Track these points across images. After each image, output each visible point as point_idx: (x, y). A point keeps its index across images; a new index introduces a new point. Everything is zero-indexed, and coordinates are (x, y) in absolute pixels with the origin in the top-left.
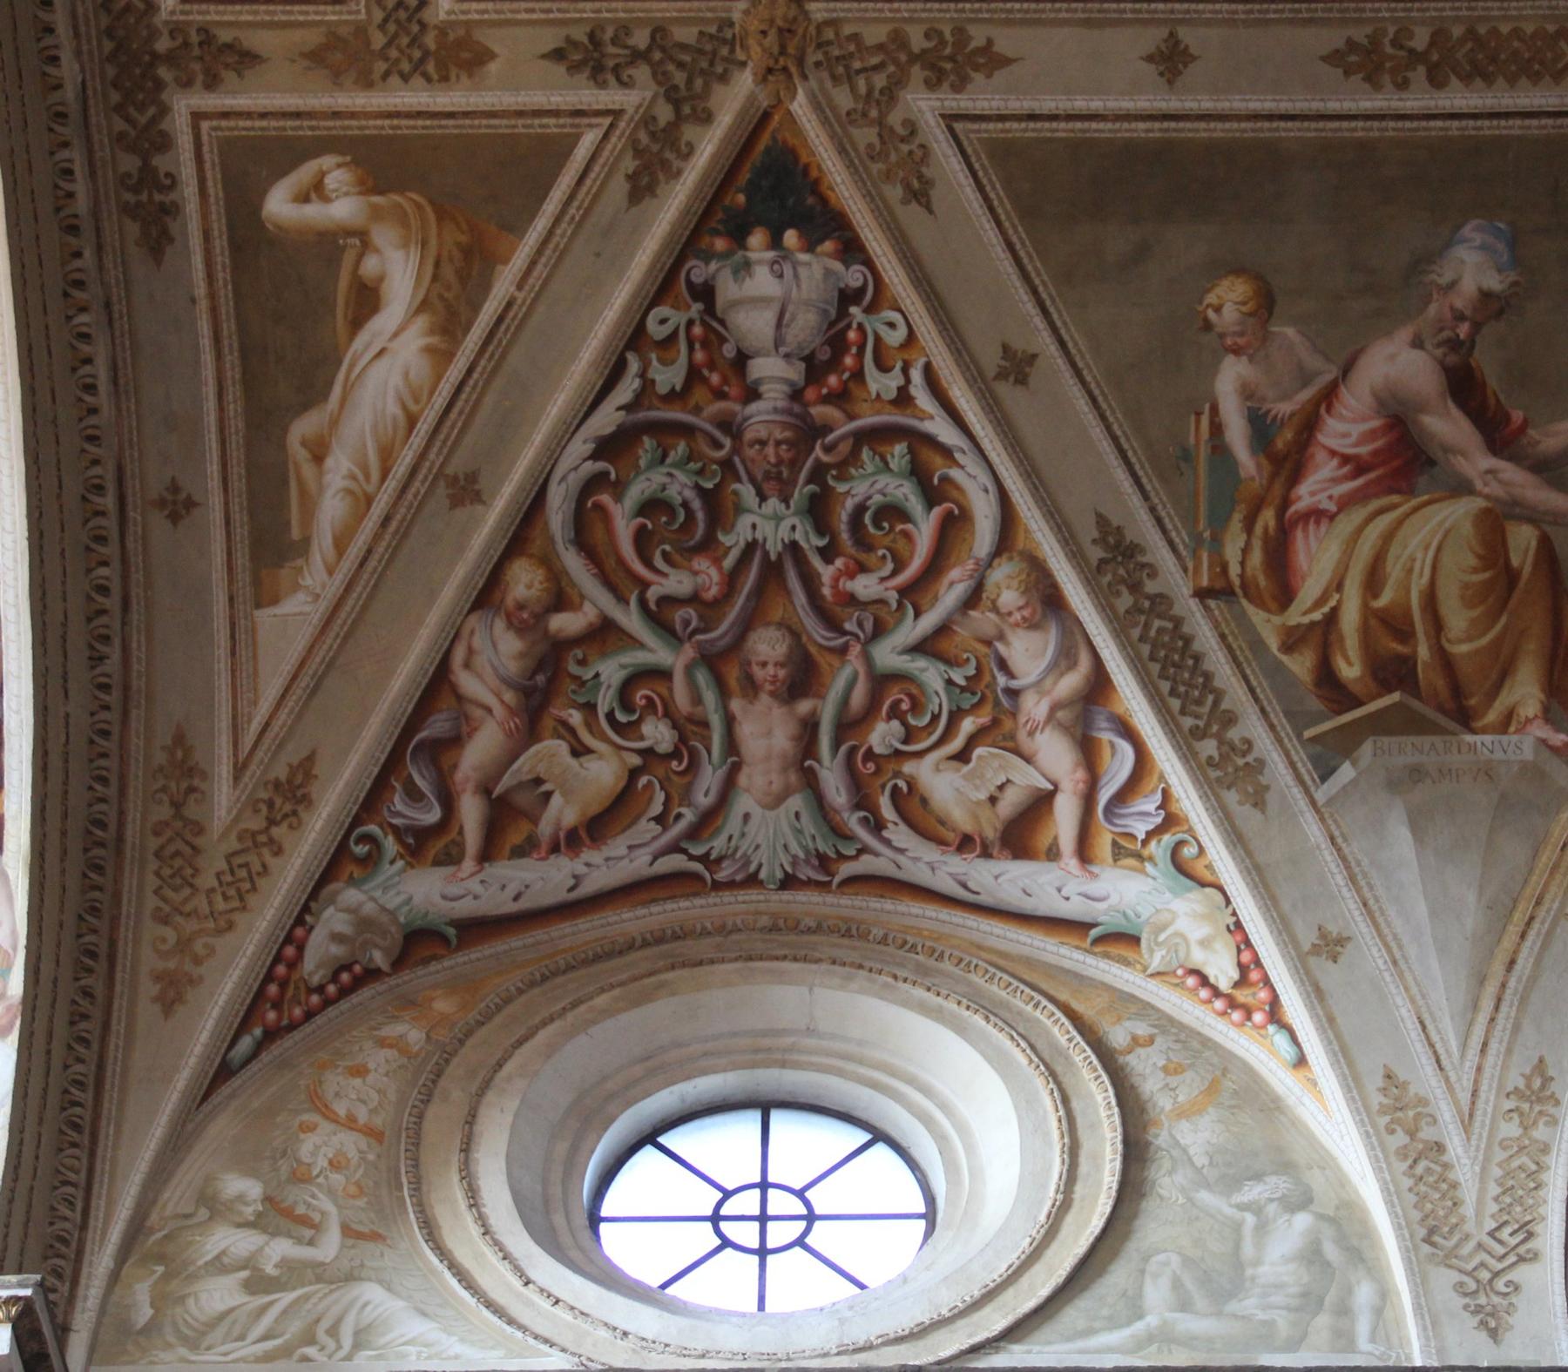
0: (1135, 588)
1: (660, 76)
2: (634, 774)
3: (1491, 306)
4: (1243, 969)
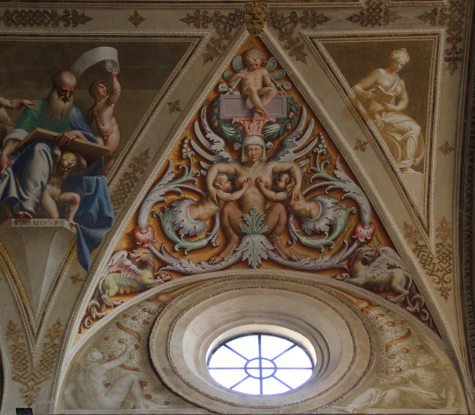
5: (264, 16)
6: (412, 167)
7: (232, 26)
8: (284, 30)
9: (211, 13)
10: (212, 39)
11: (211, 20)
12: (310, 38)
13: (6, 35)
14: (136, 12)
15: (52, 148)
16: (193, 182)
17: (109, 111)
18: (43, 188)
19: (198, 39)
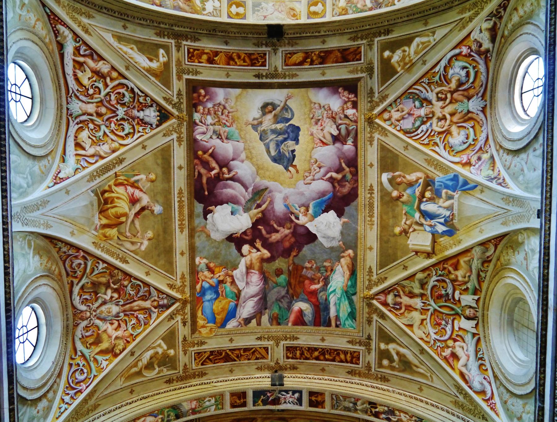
0: (116, 163)
1: (178, 102)
2: (85, 87)
3: (152, 212)
4: (62, 179)
6: (433, 36)
7: (374, 126)
9: (369, 135)
10: (379, 134)
15: (423, 202)
16: (441, 138)
17: (407, 176)
18: (440, 207)
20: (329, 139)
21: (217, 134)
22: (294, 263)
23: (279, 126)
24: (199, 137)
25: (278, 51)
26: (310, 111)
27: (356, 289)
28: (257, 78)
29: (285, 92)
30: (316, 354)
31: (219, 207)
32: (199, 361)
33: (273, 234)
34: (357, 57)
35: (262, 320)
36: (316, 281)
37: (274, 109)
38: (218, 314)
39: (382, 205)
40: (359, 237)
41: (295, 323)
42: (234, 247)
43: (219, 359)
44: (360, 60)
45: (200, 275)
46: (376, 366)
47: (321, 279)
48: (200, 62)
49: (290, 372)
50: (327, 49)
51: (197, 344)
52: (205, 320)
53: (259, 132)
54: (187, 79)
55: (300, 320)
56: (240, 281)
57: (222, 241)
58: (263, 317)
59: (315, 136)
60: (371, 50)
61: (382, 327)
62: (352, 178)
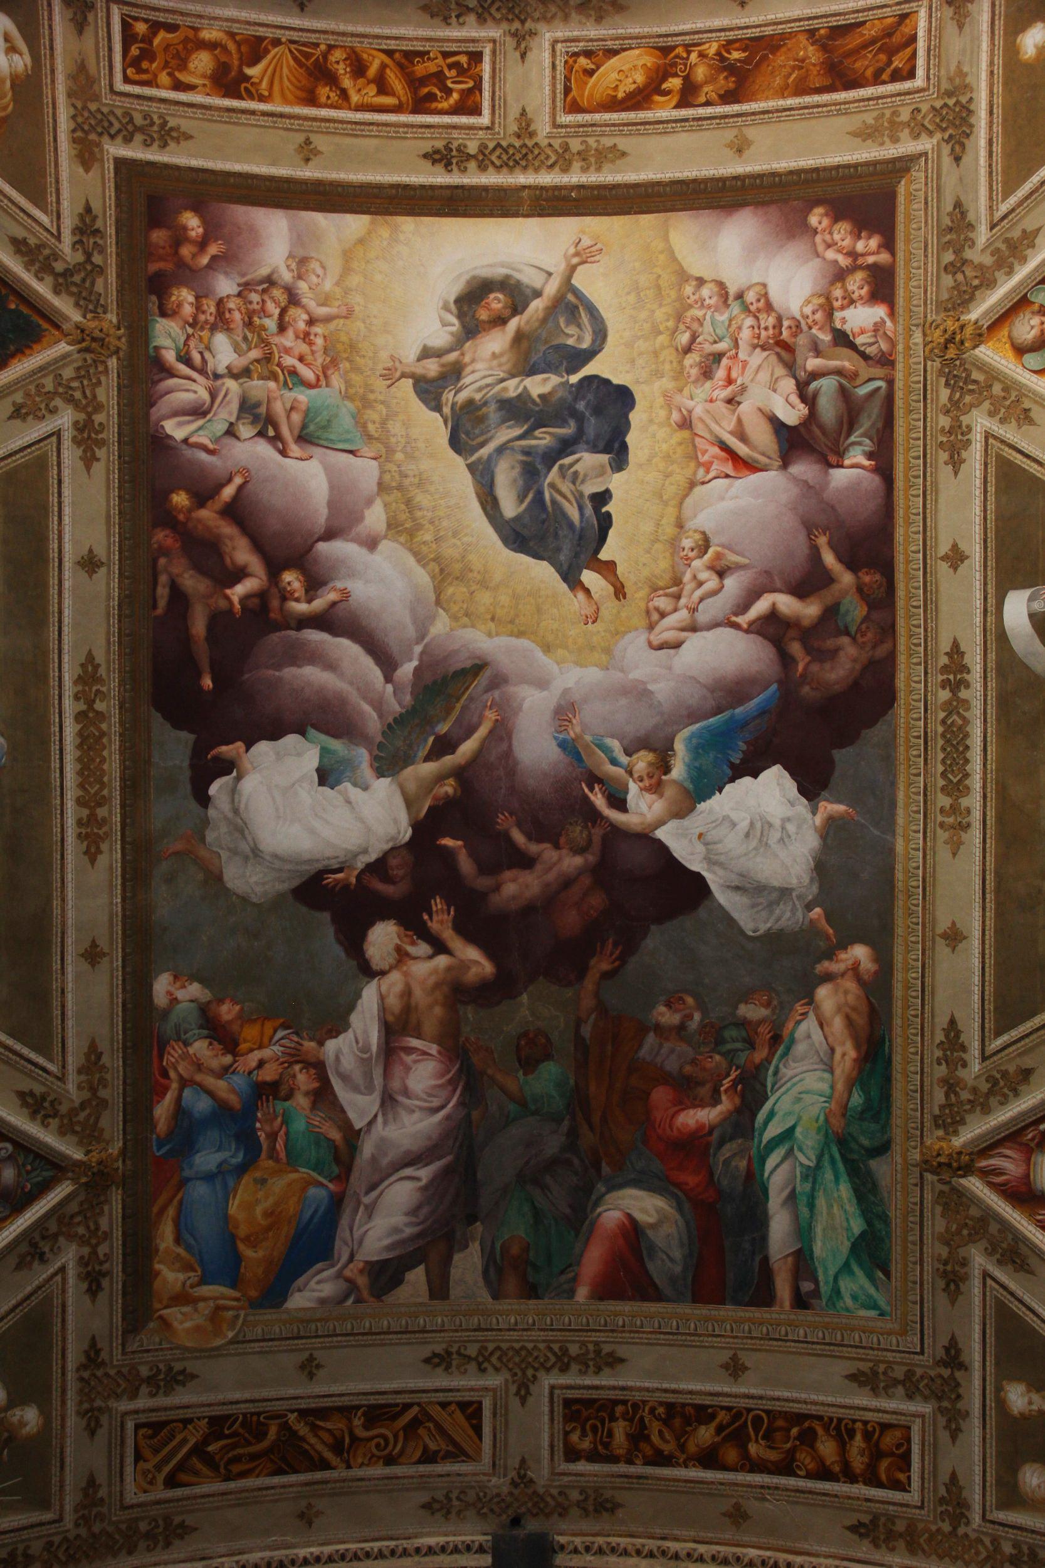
5: (949, 323)
7: (968, 380)
8: (976, 282)
9: (944, 421)
10: (991, 414)
11: (956, 419)
12: (992, 229)
13: (985, 797)
14: (942, 559)
19: (991, 441)
20: (763, 437)
21: (256, 419)
22: (602, 1009)
23: (539, 386)
24: (176, 430)
25: (533, 43)
26: (679, 318)
27: (885, 1127)
28: (439, 168)
29: (566, 231)
30: (705, 1434)
31: (263, 747)
32: (158, 1467)
33: (508, 874)
34: (897, 63)
35: (455, 1273)
36: (704, 1091)
37: (517, 309)
38: (252, 1241)
39: (1004, 738)
40: (900, 885)
41: (609, 1288)
42: (330, 931)
43: (253, 1457)
44: (911, 75)
45: (174, 1052)
46: (991, 1499)
47: (726, 1083)
48: (179, 86)
49: (585, 1526)
50: (756, 33)
51: (149, 1380)
52: (188, 1267)
53: (447, 410)
54: (121, 164)
55: (630, 1272)
56: (356, 1089)
57: (276, 903)
58: (457, 1257)
59: (699, 429)
60: (961, 26)
61: (1014, 1306)
62: (866, 619)
